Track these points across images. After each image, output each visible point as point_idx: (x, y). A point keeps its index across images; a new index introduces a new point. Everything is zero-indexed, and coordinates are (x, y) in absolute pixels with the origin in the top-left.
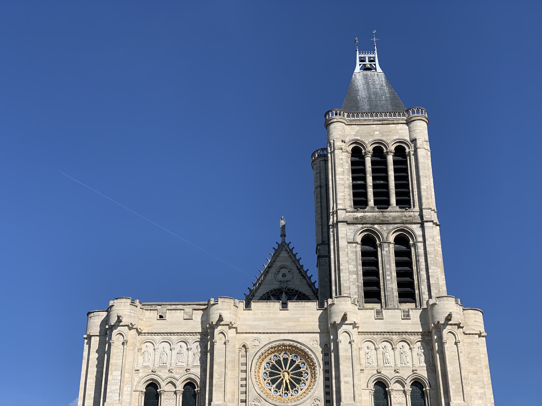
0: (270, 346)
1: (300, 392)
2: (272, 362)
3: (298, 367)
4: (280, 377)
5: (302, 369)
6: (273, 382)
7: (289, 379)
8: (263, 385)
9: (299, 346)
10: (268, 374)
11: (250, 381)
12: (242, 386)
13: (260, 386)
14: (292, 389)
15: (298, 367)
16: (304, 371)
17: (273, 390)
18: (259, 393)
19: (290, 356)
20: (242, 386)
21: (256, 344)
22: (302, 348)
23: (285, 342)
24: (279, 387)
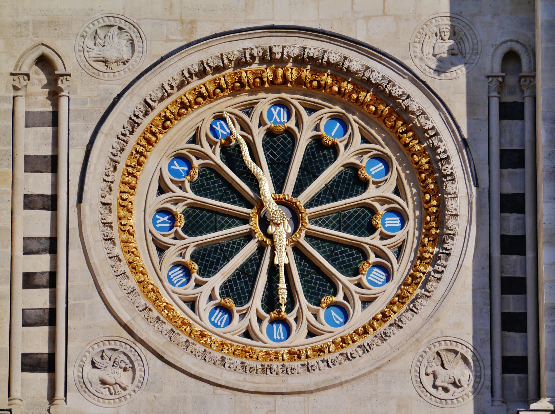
0: (191, 60)
1: (360, 316)
2: (200, 155)
3: (352, 180)
4: (249, 236)
5: (372, 192)
6: (209, 260)
7: (298, 251)
8: (152, 278)
9: (357, 62)
10: (181, 222)
11: (76, 254)
12: (30, 280)
13: (132, 282)
14: (315, 298)
15: (352, 180)
16: (384, 201)
17: (205, 307)
18: (126, 317)
19: (308, 120)
20: (30, 280)
21: (111, 53)
22: (375, 78)
23: (277, 43)
24: (238, 289)
